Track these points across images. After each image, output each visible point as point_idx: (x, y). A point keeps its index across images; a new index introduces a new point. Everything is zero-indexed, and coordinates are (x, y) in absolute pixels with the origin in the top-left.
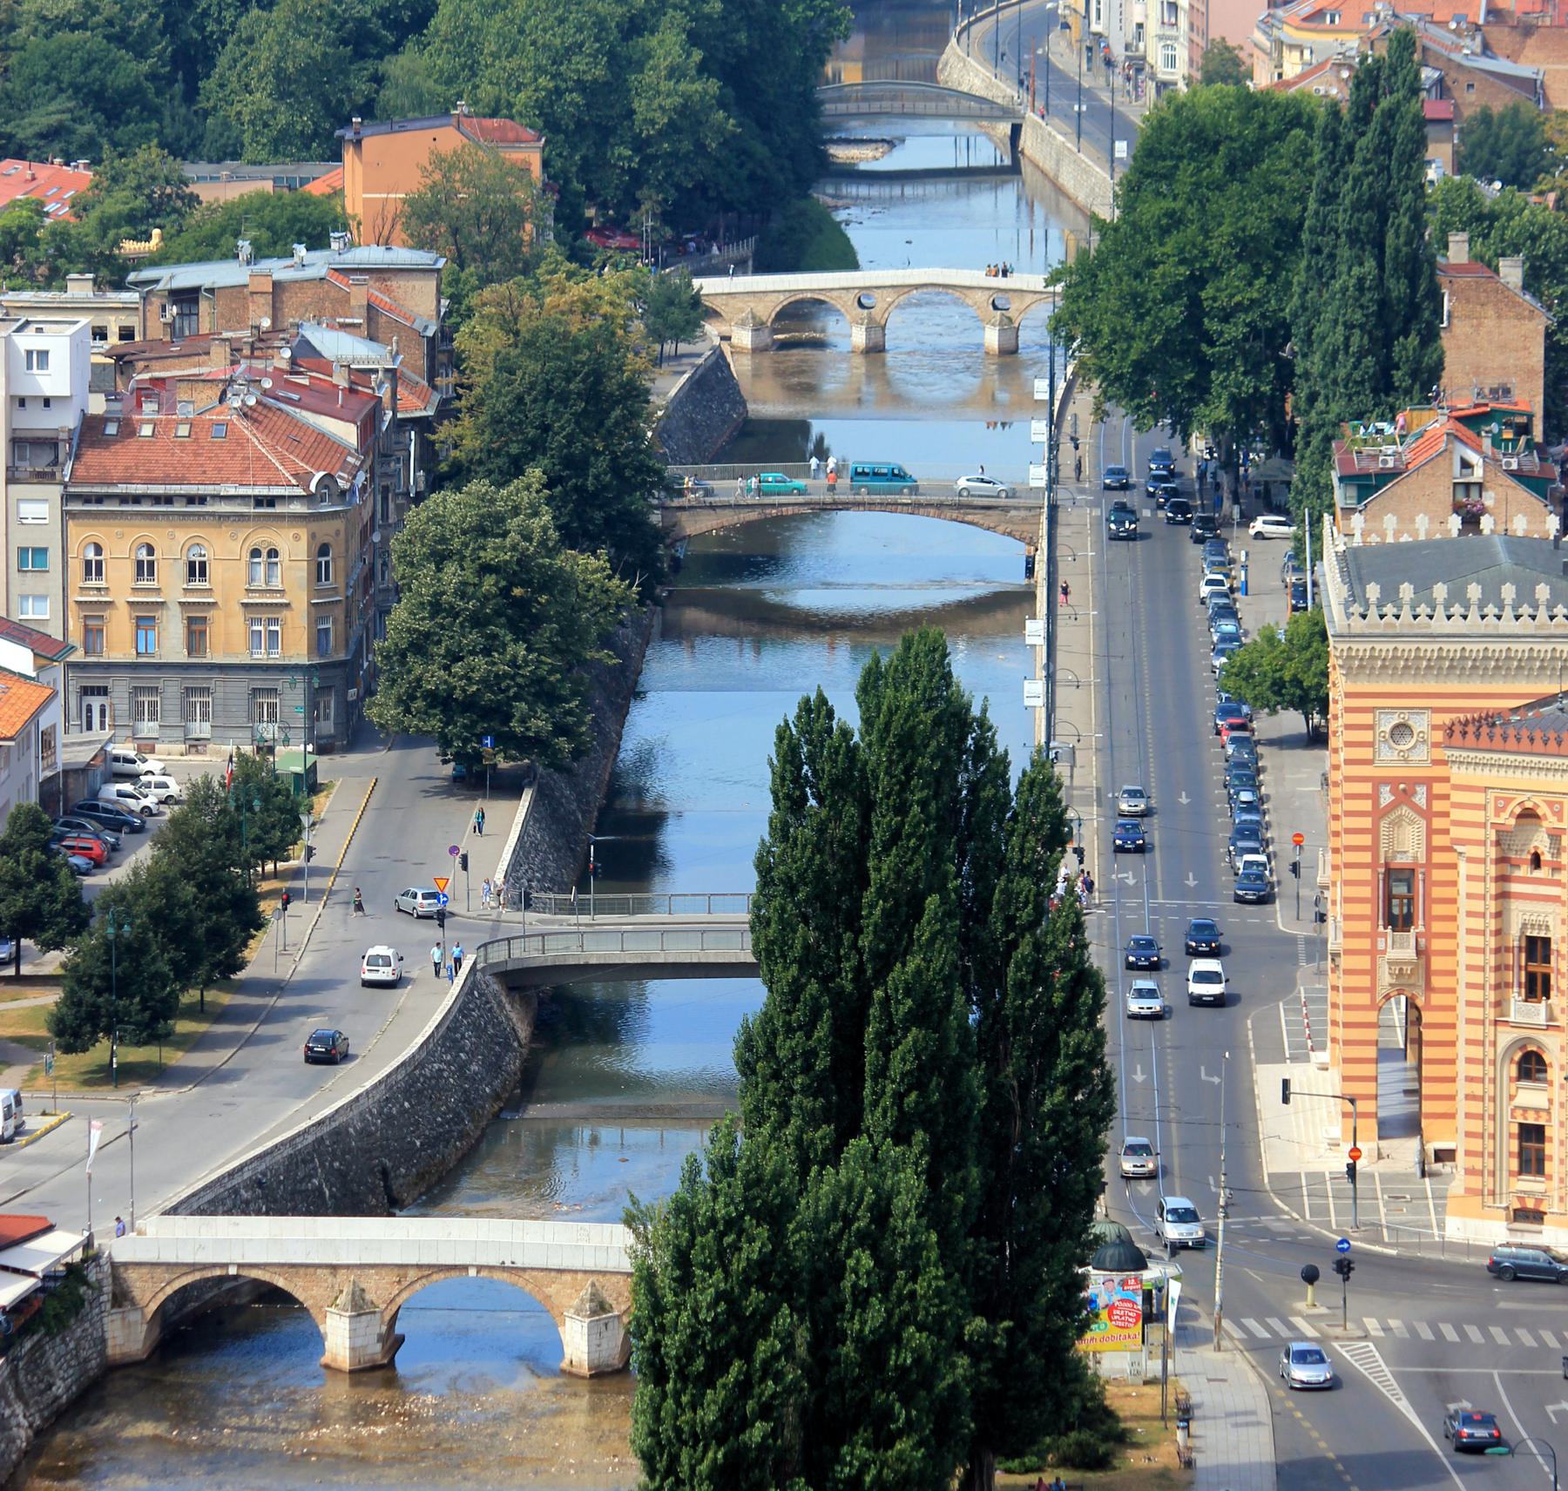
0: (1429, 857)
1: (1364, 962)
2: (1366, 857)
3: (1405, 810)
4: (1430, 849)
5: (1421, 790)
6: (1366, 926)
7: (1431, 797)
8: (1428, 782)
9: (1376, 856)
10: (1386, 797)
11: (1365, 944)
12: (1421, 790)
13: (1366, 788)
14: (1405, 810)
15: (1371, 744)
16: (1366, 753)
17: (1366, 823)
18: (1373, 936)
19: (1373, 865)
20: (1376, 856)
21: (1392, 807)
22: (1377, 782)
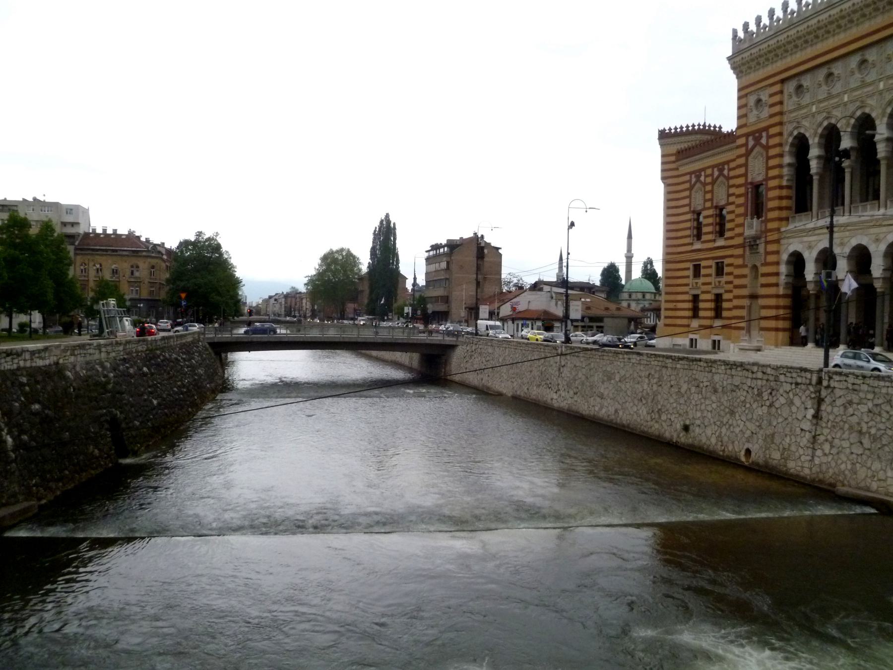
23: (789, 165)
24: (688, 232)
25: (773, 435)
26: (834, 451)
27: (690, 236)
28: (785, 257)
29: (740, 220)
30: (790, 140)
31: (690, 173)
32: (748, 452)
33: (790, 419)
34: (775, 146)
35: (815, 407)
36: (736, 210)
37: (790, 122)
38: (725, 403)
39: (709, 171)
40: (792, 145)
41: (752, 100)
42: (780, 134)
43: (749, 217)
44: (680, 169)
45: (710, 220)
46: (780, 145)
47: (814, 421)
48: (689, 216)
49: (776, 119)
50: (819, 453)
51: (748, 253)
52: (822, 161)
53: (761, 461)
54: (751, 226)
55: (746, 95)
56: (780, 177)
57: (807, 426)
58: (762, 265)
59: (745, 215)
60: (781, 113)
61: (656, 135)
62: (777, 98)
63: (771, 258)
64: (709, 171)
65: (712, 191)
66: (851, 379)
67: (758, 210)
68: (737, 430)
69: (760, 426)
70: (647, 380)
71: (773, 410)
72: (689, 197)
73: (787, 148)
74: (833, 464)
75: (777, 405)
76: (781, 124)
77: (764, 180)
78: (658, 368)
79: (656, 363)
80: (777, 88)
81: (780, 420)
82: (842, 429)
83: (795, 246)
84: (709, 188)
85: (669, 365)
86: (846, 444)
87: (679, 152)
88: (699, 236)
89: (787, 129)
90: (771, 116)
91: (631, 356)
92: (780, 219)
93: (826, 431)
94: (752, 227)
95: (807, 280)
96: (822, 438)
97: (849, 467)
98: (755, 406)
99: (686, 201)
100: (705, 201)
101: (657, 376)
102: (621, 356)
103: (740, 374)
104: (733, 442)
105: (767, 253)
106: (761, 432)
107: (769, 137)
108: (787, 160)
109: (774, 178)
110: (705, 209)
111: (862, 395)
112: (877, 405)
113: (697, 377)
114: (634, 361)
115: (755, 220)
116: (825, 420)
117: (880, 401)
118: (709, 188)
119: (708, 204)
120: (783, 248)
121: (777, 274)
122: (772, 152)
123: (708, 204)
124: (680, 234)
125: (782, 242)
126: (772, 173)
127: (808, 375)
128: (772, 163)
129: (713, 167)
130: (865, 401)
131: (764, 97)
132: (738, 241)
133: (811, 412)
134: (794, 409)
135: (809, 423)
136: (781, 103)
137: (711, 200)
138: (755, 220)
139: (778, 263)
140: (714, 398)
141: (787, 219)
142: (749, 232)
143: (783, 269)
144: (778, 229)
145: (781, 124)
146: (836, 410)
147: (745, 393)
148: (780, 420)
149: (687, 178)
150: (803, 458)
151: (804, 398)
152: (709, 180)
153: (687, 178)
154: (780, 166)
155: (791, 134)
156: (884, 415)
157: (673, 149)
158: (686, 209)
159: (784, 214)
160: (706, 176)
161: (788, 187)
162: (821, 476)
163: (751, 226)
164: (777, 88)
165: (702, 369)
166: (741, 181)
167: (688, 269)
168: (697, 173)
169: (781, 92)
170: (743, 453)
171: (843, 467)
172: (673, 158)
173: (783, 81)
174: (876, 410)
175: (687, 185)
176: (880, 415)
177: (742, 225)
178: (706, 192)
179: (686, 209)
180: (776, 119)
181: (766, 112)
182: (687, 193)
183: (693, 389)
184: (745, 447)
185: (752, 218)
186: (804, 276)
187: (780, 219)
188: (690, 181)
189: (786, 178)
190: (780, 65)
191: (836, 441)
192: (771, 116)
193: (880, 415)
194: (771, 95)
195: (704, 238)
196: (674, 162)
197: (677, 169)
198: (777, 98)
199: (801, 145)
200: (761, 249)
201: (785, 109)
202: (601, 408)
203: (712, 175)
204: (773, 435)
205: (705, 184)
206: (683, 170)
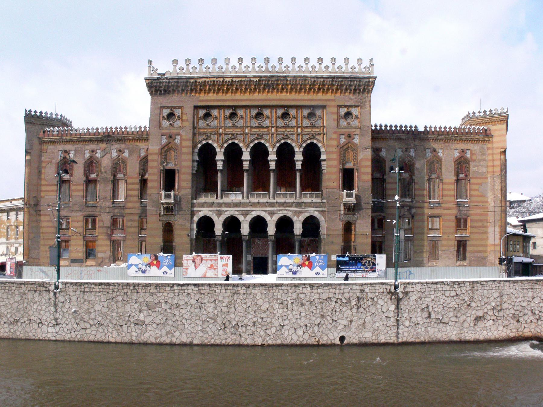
33: (377, 313)
35: (396, 303)
38: (314, 311)
47: (396, 311)
66: (419, 286)
70: (213, 305)
71: (361, 310)
78: (226, 295)
79: (223, 291)
82: (417, 312)
83: (203, 211)
85: (241, 292)
91: (184, 288)
95: (269, 234)
98: (344, 309)
101: (226, 300)
102: (168, 288)
103: (328, 291)
111: (426, 293)
112: (437, 297)
113: (279, 297)
114: (190, 291)
117: (438, 295)
127: (388, 287)
130: (429, 296)
135: (392, 313)
140: (301, 309)
146: (411, 303)
147: (334, 303)
151: (386, 300)
156: (442, 301)
165: (285, 291)
174: (436, 299)
176: (439, 301)
183: (276, 306)
186: (293, 232)
193: (439, 301)
202: (142, 333)
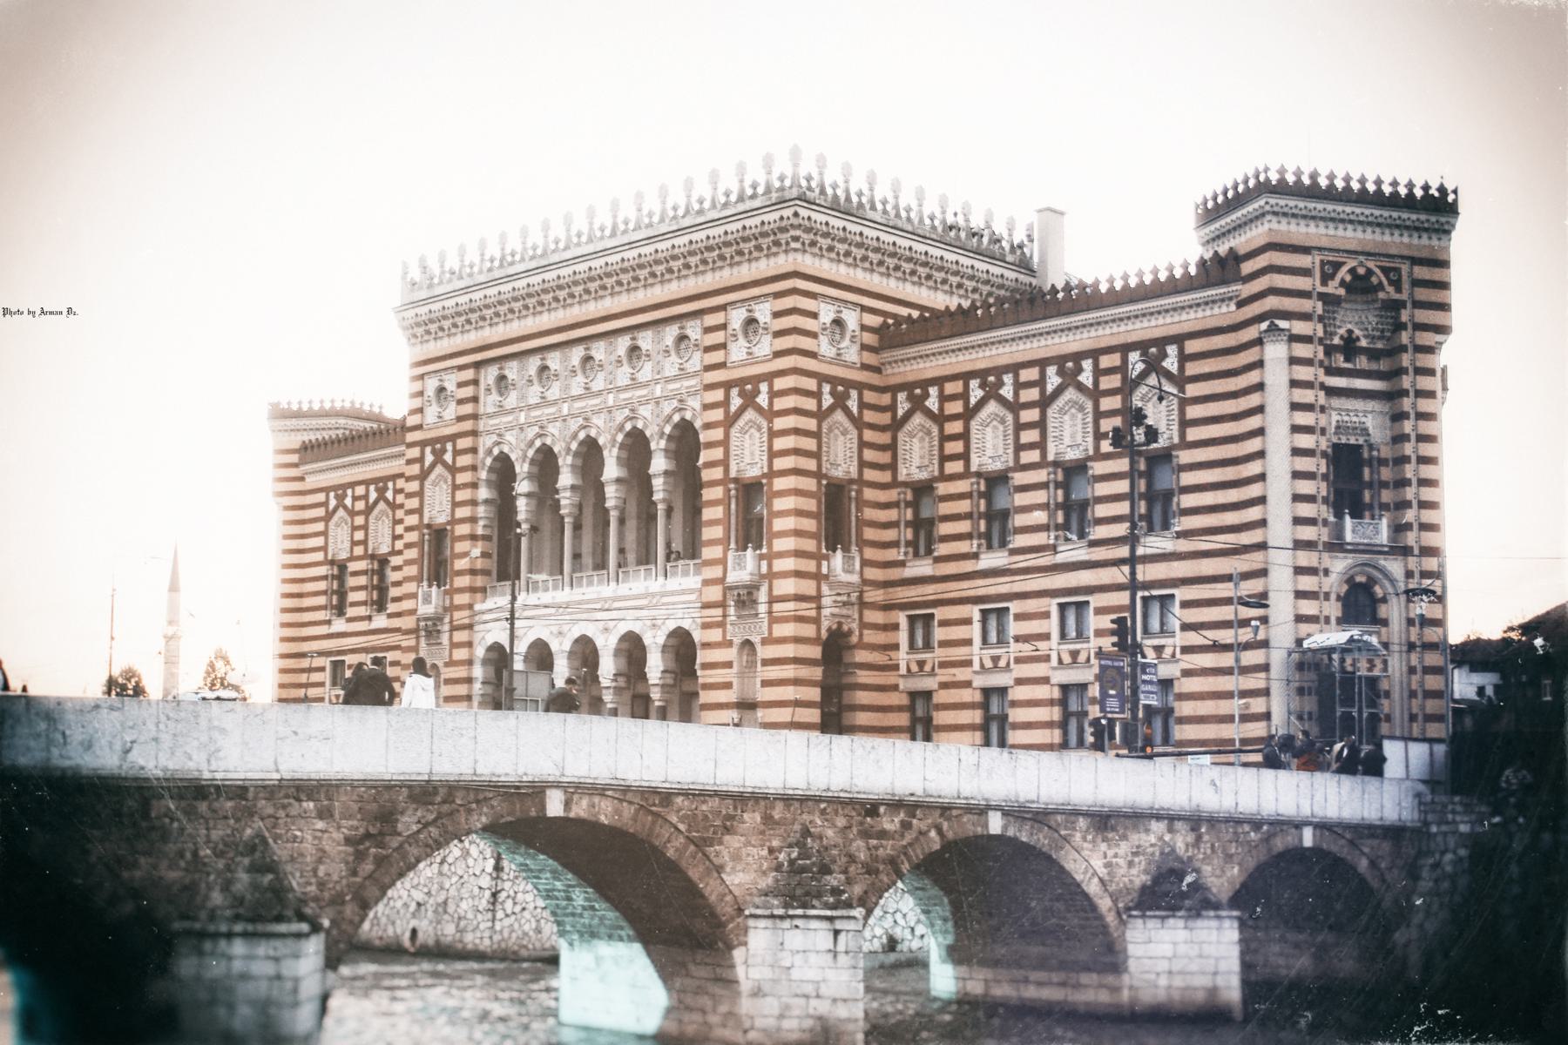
0: (860, 473)
1: (808, 587)
2: (811, 465)
3: (839, 416)
4: (863, 464)
5: (854, 394)
6: (810, 545)
7: (863, 405)
8: (861, 387)
9: (819, 466)
10: (828, 401)
11: (810, 566)
12: (854, 394)
13: (718, 395)
14: (839, 416)
15: (723, 346)
16: (717, 357)
17: (811, 424)
18: (818, 557)
19: (818, 475)
20: (819, 466)
21: (832, 409)
22: (822, 378)
23: (486, 501)
24: (322, 600)
25: (445, 903)
26: (518, 909)
27: (324, 608)
28: (480, 652)
29: (410, 587)
30: (489, 461)
31: (326, 490)
32: (414, 932)
34: (463, 469)
36: (405, 569)
37: (489, 433)
39: (360, 490)
40: (491, 470)
41: (431, 384)
42: (474, 450)
43: (425, 583)
44: (309, 479)
45: (362, 580)
46: (474, 468)
48: (323, 570)
49: (467, 425)
50: (500, 914)
51: (423, 642)
52: (534, 502)
53: (431, 942)
54: (427, 600)
55: (422, 377)
56: (473, 520)
57: (486, 881)
58: (447, 665)
59: (418, 579)
60: (475, 417)
61: (265, 412)
62: (468, 392)
63: (461, 654)
64: (360, 490)
65: (365, 527)
67: (438, 570)
68: (399, 904)
69: (429, 894)
71: (446, 867)
72: (325, 533)
73: (483, 475)
74: (516, 926)
75: (450, 860)
76: (474, 433)
77: (448, 523)
80: (469, 374)
81: (455, 879)
84: (359, 520)
86: (529, 897)
87: (306, 448)
88: (340, 610)
89: (485, 442)
90: (460, 419)
92: (472, 590)
93: (507, 885)
94: (429, 602)
96: (503, 895)
97: (534, 925)
99: (319, 541)
100: (354, 543)
104: (393, 923)
105: (454, 645)
106: (431, 901)
107: (457, 453)
108: (484, 493)
109: (462, 521)
110: (352, 558)
115: (434, 588)
116: (506, 870)
118: (359, 520)
119: (359, 550)
120: (477, 638)
121: (469, 680)
122: (463, 478)
123: (359, 550)
124: (308, 602)
125: (476, 628)
126: (462, 512)
128: (462, 495)
129: (366, 483)
131: (450, 382)
132: (408, 623)
133: (492, 862)
134: (470, 862)
136: (475, 399)
137: (365, 542)
138: (434, 588)
139: (470, 663)
141: (484, 590)
142: (426, 610)
143: (478, 672)
144: (470, 606)
145: (474, 433)
148: (455, 879)
149: (321, 497)
150: (482, 926)
152: (360, 505)
153: (321, 497)
154: (473, 503)
155: (490, 452)
157: (296, 441)
158: (319, 556)
159: (479, 581)
160: (355, 499)
161: (486, 538)
162: (503, 945)
163: (427, 600)
164: (469, 374)
166: (412, 520)
167: (322, 669)
168: (340, 489)
169: (475, 382)
170: (408, 935)
171: (526, 928)
172: (295, 458)
173: (477, 365)
175: (321, 512)
177: (414, 596)
178: (354, 528)
179: (319, 556)
180: (467, 425)
181: (451, 411)
182: (320, 527)
184: (410, 927)
185: (430, 586)
187: (472, 590)
188: (325, 504)
189: (481, 523)
190: (472, 338)
191: (520, 896)
192: (460, 419)
194: (460, 385)
195: (351, 612)
196: (296, 465)
197: (302, 479)
198: (468, 392)
199: (504, 471)
200: (445, 638)
201: (481, 411)
203: (366, 497)
204: (445, 903)
205: (352, 513)
206: (312, 482)
